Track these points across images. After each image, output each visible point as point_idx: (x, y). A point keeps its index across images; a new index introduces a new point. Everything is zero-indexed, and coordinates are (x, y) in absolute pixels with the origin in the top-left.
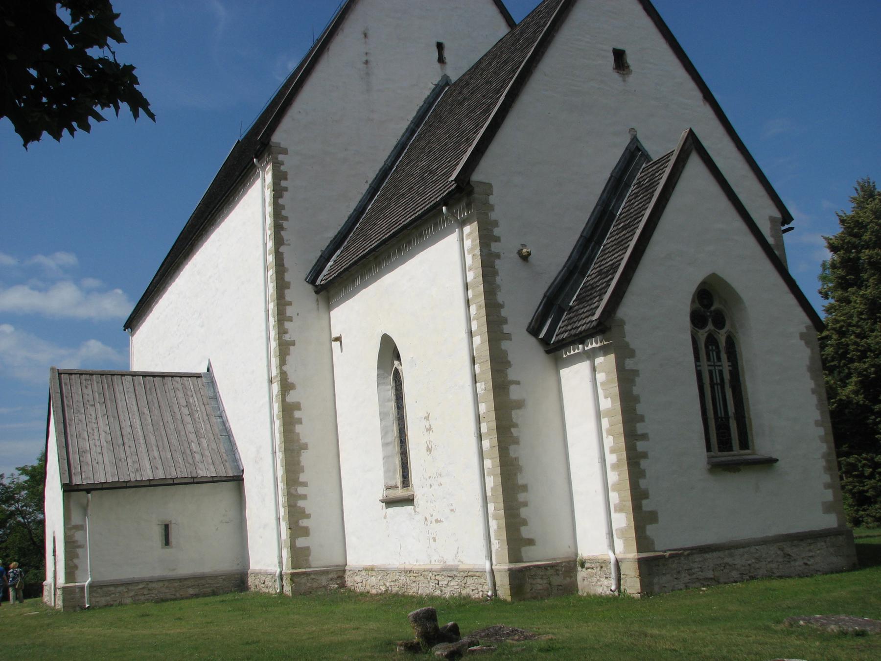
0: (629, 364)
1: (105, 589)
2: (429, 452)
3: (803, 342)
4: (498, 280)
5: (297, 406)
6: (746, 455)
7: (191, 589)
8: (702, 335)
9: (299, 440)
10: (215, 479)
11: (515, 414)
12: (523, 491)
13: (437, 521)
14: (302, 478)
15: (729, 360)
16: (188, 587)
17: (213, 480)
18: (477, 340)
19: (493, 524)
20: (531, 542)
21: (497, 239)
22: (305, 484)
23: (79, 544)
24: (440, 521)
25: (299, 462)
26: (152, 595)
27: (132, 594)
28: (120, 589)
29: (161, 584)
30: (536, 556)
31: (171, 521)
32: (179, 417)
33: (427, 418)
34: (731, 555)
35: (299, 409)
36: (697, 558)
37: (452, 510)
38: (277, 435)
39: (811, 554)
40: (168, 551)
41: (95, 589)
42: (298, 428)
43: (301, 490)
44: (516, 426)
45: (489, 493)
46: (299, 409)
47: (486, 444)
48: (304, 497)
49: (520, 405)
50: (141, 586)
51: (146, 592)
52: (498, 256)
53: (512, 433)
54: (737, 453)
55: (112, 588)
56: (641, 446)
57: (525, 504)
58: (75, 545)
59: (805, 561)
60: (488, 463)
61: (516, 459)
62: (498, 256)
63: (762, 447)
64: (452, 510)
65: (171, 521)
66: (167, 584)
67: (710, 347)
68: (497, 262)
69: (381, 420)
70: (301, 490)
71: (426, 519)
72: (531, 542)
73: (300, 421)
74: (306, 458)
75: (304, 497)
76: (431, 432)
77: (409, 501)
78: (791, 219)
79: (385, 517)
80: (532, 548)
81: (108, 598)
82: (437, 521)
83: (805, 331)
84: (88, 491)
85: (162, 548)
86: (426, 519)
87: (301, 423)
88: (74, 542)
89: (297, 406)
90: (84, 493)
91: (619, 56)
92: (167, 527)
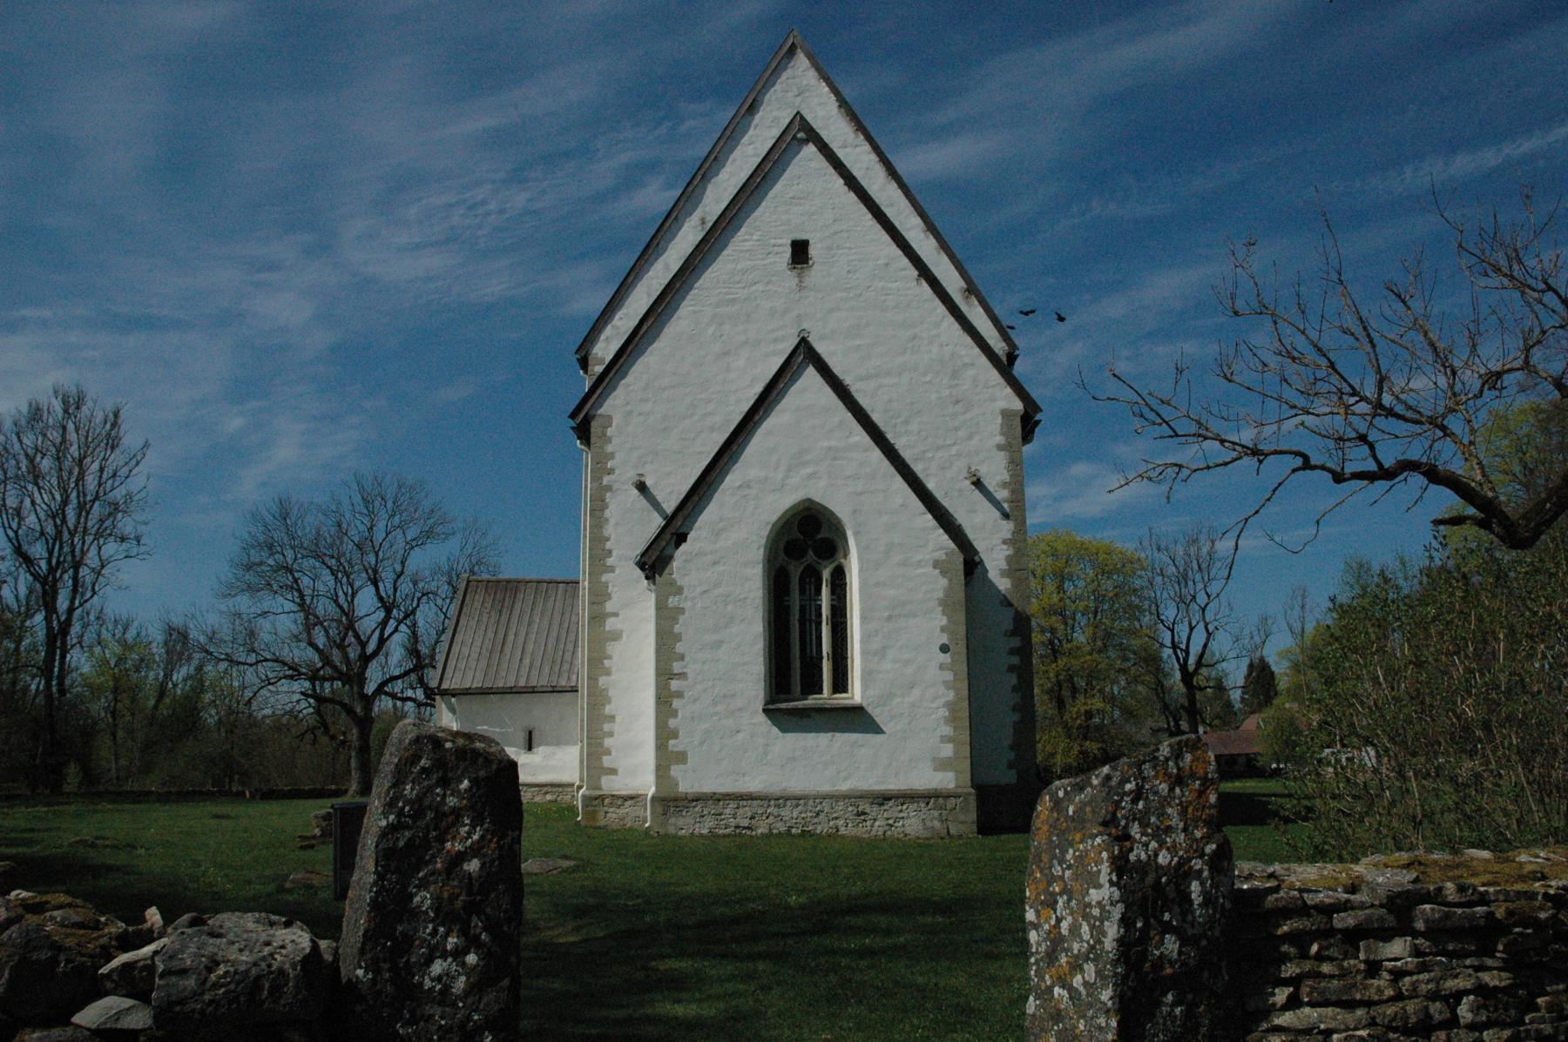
0: (673, 601)
3: (937, 571)
4: (607, 513)
6: (841, 699)
8: (795, 570)
11: (611, 648)
12: (610, 722)
15: (833, 592)
21: (611, 472)
32: (566, 625)
34: (778, 806)
36: (733, 805)
39: (901, 815)
44: (610, 658)
49: (616, 636)
52: (609, 488)
53: (603, 664)
54: (826, 696)
56: (675, 685)
57: (611, 734)
59: (891, 822)
61: (606, 690)
62: (609, 488)
63: (856, 693)
67: (808, 580)
68: (608, 495)
72: (613, 771)
78: (1038, 409)
80: (612, 777)
83: (944, 557)
91: (800, 252)
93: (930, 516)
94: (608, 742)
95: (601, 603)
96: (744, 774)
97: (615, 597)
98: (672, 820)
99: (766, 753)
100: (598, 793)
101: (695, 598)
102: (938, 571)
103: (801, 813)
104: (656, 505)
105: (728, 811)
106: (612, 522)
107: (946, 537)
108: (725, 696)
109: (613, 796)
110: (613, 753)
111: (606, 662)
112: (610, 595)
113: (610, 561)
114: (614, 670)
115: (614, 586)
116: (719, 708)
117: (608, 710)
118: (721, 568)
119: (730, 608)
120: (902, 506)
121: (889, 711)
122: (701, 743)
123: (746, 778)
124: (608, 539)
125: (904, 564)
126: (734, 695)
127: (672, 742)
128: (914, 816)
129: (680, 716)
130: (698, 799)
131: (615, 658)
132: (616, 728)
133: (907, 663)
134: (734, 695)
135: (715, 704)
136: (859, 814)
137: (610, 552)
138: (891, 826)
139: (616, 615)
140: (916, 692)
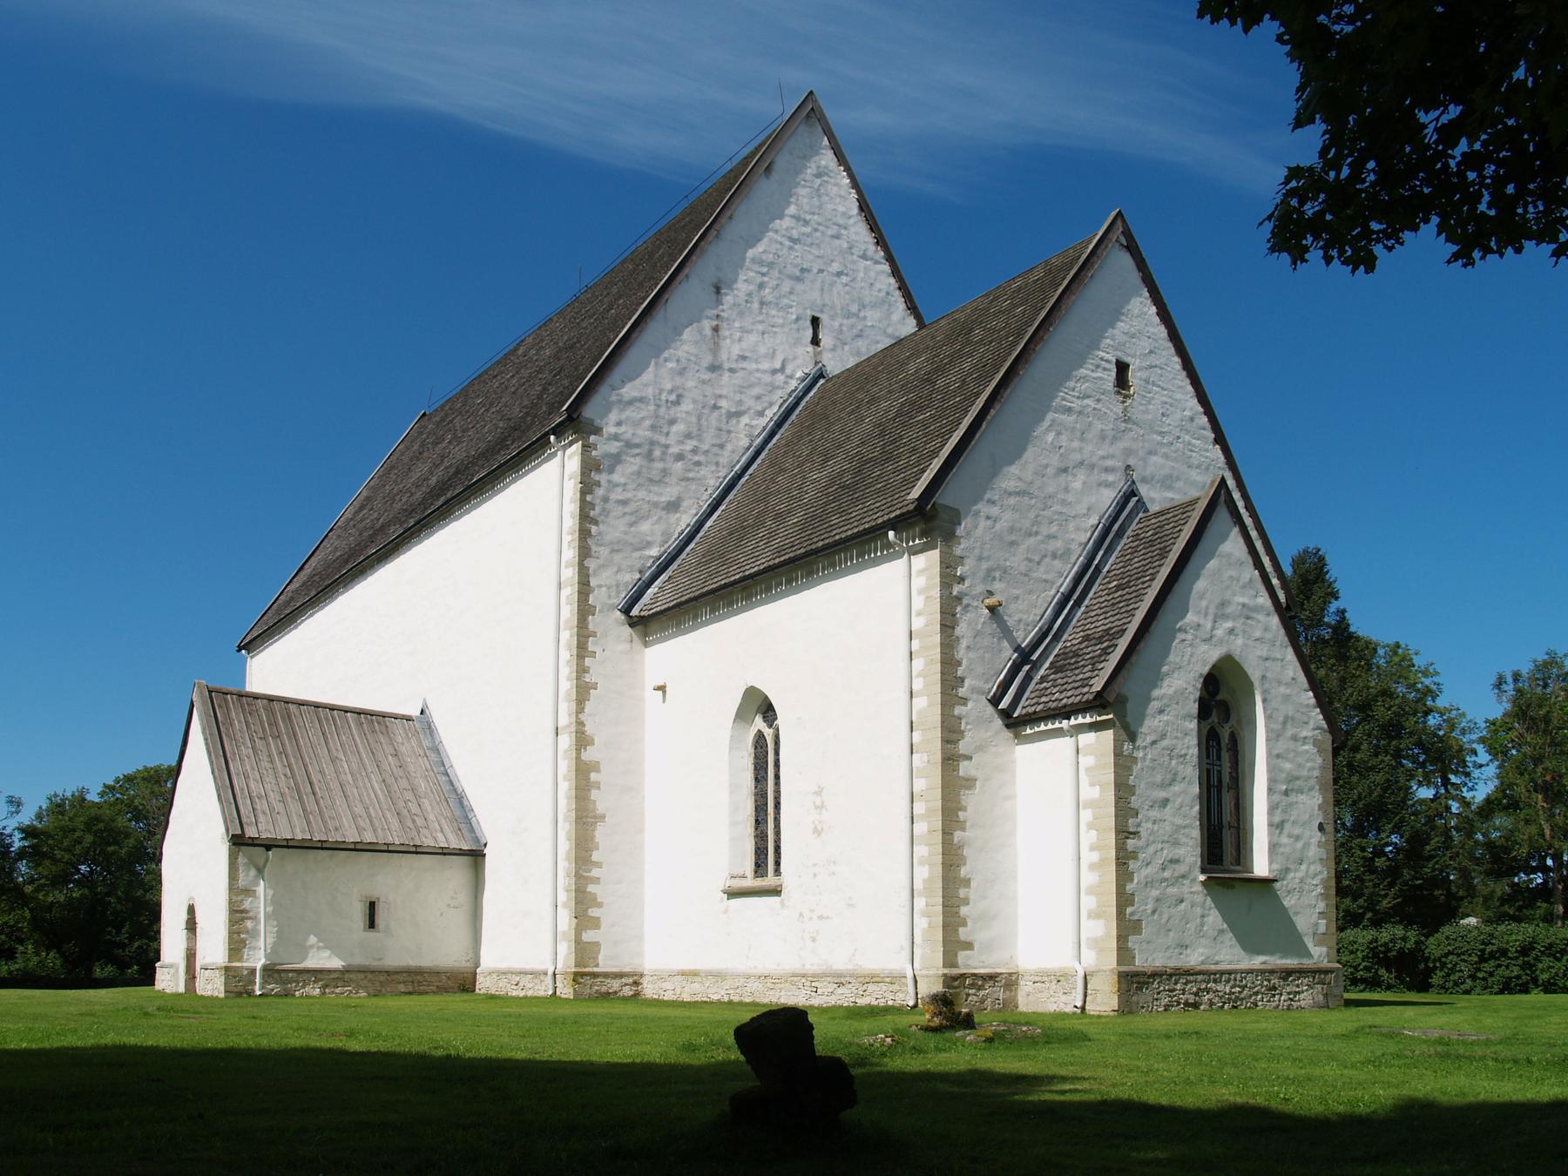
2: (816, 835)
5: (596, 767)
9: (595, 809)
10: (445, 851)
13: (821, 917)
14: (595, 856)
17: (444, 852)
18: (920, 703)
19: (921, 923)
20: (969, 946)
22: (599, 865)
24: (828, 918)
25: (593, 838)
30: (973, 962)
33: (819, 793)
35: (598, 770)
37: (850, 905)
38: (563, 802)
42: (594, 794)
43: (595, 872)
45: (918, 885)
46: (598, 770)
47: (921, 828)
48: (596, 880)
57: (966, 902)
60: (921, 850)
61: (960, 847)
64: (850, 905)
69: (731, 793)
70: (595, 872)
71: (801, 915)
72: (969, 946)
73: (597, 786)
74: (600, 833)
75: (596, 880)
76: (824, 811)
77: (775, 892)
79: (726, 912)
82: (821, 917)
86: (801, 915)
87: (599, 788)
89: (596, 767)
93: (1311, 694)
94: (964, 910)
95: (955, 742)
96: (1187, 947)
97: (968, 735)
98: (1134, 998)
99: (1202, 925)
100: (955, 971)
101: (1145, 747)
102: (1316, 750)
103: (1232, 988)
104: (1006, 632)
105: (1179, 987)
106: (964, 644)
107: (1321, 717)
108: (1171, 861)
109: (975, 975)
110: (969, 924)
111: (960, 813)
112: (963, 732)
113: (962, 692)
114: (968, 824)
115: (967, 723)
116: (1166, 874)
117: (963, 872)
118: (1165, 718)
119: (1174, 762)
120: (1293, 679)
121: (1287, 886)
122: (1154, 912)
123: (1189, 951)
124: (959, 664)
125: (1295, 738)
126: (1177, 861)
127: (1129, 910)
128: (1307, 990)
129: (1136, 881)
130: (1155, 975)
131: (969, 809)
132: (972, 893)
133: (1298, 838)
134: (1177, 861)
135: (1163, 869)
136: (1270, 989)
137: (962, 680)
138: (1291, 1000)
139: (969, 758)
140: (1303, 867)
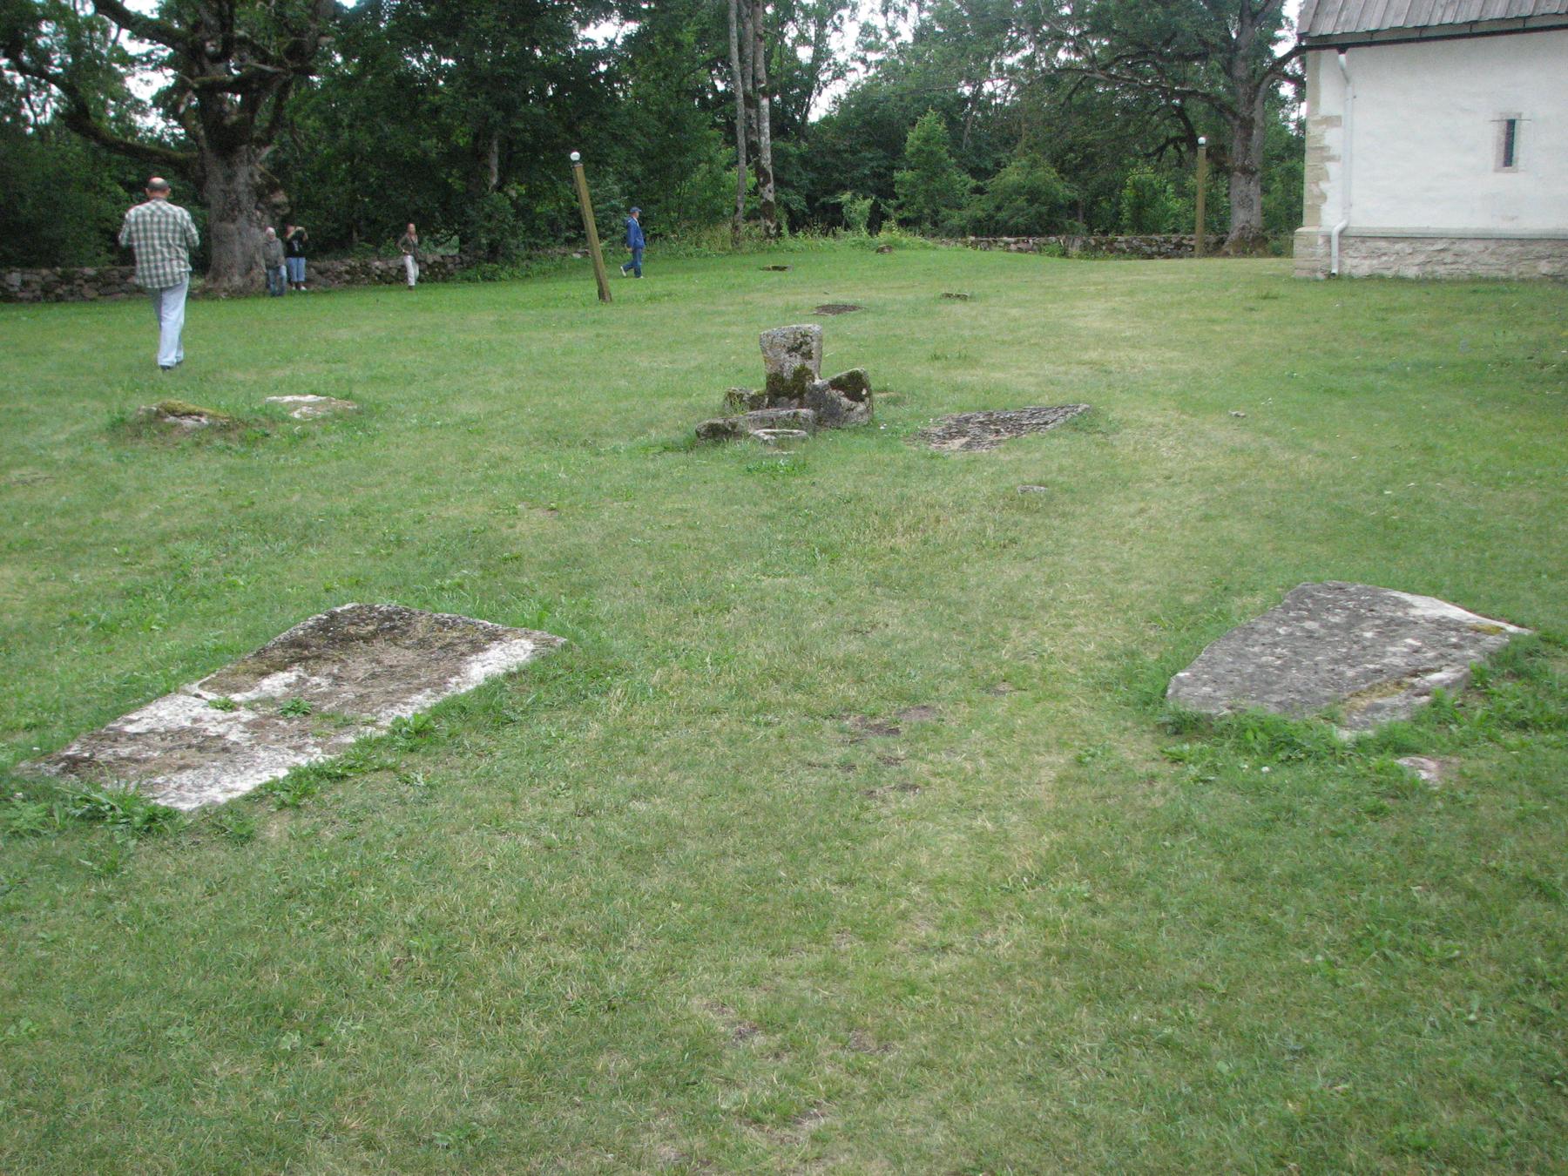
1: (1371, 244)
7: (1543, 262)
16: (1539, 258)
23: (1332, 153)
26: (1462, 267)
27: (1421, 258)
28: (1398, 247)
29: (1480, 246)
31: (1520, 115)
40: (1506, 177)
41: (1352, 241)
50: (1439, 246)
51: (1449, 258)
55: (1383, 244)
58: (1325, 154)
65: (1520, 115)
66: (1492, 246)
81: (1375, 262)
84: (1342, 48)
85: (1496, 171)
88: (1322, 148)
90: (1335, 52)
92: (1511, 124)
